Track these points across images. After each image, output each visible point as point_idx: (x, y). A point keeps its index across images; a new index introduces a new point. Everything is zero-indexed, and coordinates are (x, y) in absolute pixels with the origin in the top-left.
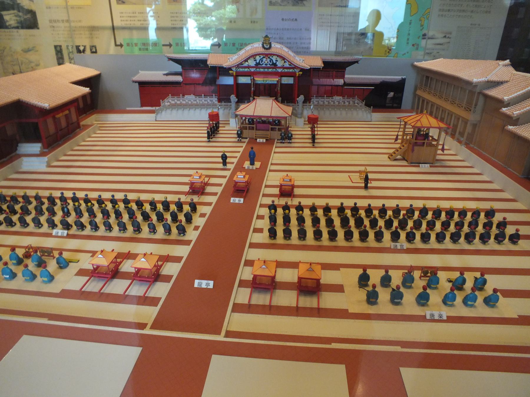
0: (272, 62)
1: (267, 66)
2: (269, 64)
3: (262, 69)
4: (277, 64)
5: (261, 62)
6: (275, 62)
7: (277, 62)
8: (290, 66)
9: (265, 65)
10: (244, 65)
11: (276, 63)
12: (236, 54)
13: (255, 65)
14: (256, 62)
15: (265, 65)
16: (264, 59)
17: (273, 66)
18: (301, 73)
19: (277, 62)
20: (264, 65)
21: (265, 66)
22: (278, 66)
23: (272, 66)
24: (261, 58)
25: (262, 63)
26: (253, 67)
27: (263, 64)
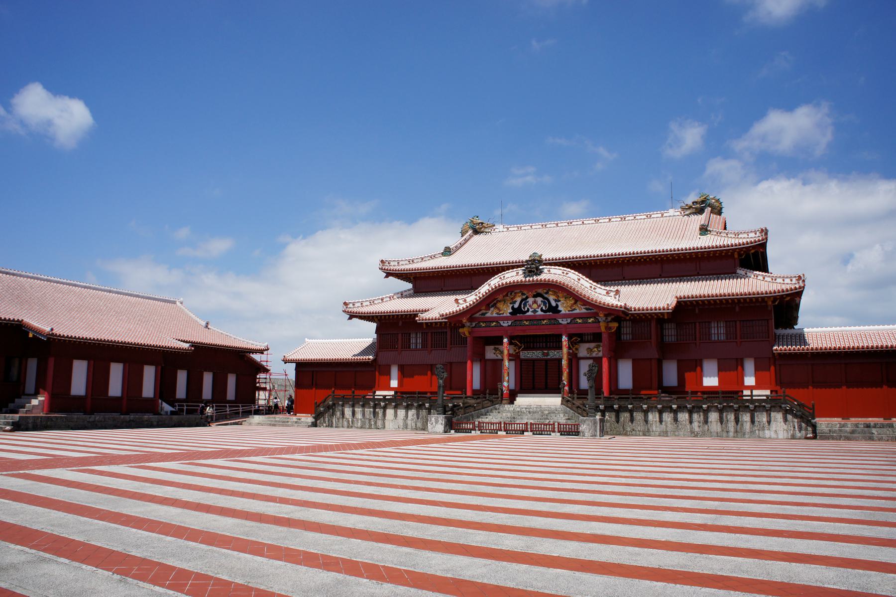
0: (547, 305)
1: (537, 314)
2: (542, 310)
3: (527, 321)
4: (560, 308)
5: (522, 306)
6: (554, 304)
7: (559, 304)
8: (589, 311)
9: (532, 312)
10: (488, 315)
11: (557, 306)
14: (513, 308)
15: (532, 312)
16: (531, 300)
17: (551, 313)
18: (615, 325)
19: (559, 304)
20: (530, 313)
21: (532, 314)
22: (561, 313)
23: (548, 313)
24: (524, 297)
25: (526, 309)
26: (506, 318)
27: (528, 310)
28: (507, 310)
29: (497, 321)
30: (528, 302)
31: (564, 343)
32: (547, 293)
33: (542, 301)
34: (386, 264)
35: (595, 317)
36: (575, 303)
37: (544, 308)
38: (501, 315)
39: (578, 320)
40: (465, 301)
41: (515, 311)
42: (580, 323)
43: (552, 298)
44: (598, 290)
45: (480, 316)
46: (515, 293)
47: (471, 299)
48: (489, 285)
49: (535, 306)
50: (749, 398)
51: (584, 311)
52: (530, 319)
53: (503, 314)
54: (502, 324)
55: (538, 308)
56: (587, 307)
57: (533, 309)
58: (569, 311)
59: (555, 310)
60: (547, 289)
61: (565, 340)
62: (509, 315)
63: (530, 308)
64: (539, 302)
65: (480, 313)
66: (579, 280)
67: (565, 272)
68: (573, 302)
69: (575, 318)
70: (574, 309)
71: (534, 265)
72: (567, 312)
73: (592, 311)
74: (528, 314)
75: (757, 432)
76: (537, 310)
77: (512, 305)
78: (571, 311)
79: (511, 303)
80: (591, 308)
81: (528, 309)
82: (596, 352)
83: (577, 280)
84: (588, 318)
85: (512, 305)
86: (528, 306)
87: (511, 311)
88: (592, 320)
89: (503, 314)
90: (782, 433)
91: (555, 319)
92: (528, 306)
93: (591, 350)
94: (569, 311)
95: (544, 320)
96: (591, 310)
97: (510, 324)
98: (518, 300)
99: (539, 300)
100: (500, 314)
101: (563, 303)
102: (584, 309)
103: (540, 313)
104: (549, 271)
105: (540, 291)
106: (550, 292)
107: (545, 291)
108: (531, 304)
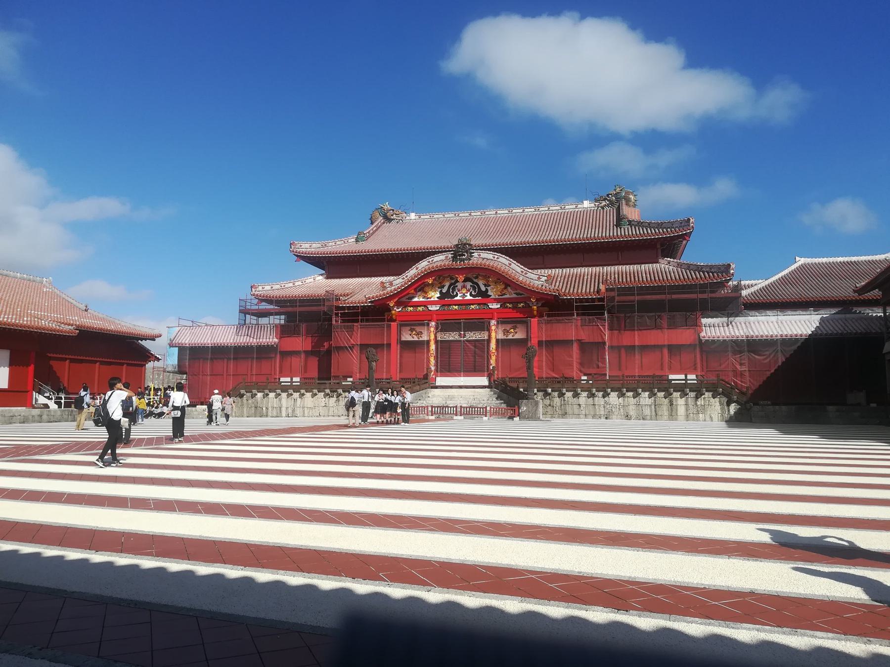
0: (477, 290)
1: (466, 298)
2: (471, 295)
3: (455, 305)
4: (489, 293)
5: (451, 290)
6: (483, 289)
7: (489, 288)
8: (520, 296)
11: (487, 289)
12: (400, 277)
13: (437, 297)
14: (441, 292)
17: (480, 298)
19: (489, 288)
21: (461, 298)
22: (491, 297)
23: (477, 298)
24: (453, 281)
25: (455, 293)
27: (457, 295)
28: (435, 295)
29: (425, 306)
30: (457, 286)
31: (493, 328)
32: (477, 278)
33: (471, 286)
34: (297, 247)
35: (525, 302)
36: (505, 288)
37: (473, 293)
38: (429, 300)
39: (508, 305)
40: (391, 284)
41: (443, 296)
42: (510, 308)
43: (481, 283)
44: (529, 275)
45: (407, 300)
46: (444, 278)
47: (397, 282)
48: (417, 269)
49: (464, 291)
50: (684, 382)
51: (515, 296)
52: (458, 303)
53: (431, 298)
54: (429, 308)
55: (467, 293)
56: (518, 291)
57: (462, 294)
58: (499, 296)
59: (485, 294)
60: (477, 274)
61: (494, 325)
62: (436, 299)
63: (458, 293)
64: (469, 287)
65: (407, 297)
66: (510, 264)
67: (496, 257)
68: (503, 287)
69: (505, 303)
70: (504, 294)
71: (461, 250)
72: (497, 297)
73: (523, 296)
74: (456, 298)
75: (691, 415)
76: (466, 294)
77: (440, 290)
78: (502, 295)
79: (439, 288)
80: (521, 292)
81: (457, 294)
82: (512, 334)
83: (508, 265)
84: (518, 303)
85: (440, 290)
86: (457, 291)
87: (438, 295)
88: (522, 304)
89: (431, 298)
90: (717, 416)
91: (485, 304)
92: (457, 291)
93: (508, 332)
94: (499, 296)
95: (473, 305)
96: (521, 294)
97: (438, 308)
98: (447, 284)
99: (469, 284)
100: (428, 298)
101: (493, 289)
102: (515, 293)
103: (468, 297)
104: (480, 255)
105: (469, 276)
106: (479, 277)
107: (474, 275)
108: (460, 289)
